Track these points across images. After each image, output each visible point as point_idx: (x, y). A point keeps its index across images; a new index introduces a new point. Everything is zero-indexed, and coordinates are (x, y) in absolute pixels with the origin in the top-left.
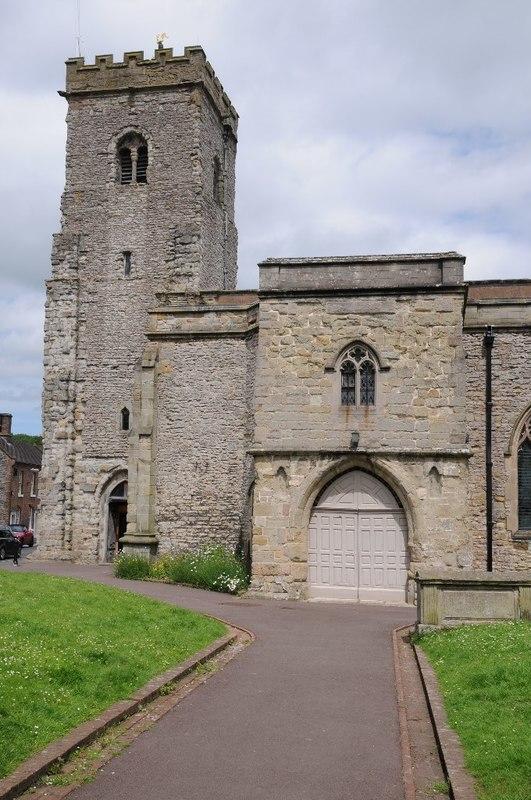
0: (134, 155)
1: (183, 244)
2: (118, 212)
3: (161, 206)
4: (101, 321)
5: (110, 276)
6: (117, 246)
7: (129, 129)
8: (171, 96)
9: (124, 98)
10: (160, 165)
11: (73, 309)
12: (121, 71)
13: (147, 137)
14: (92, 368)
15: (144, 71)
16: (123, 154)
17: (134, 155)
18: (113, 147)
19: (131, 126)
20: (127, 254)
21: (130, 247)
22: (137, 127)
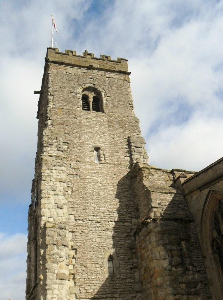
0: (91, 100)
1: (136, 147)
2: (87, 124)
3: (116, 125)
4: (85, 188)
5: (87, 160)
6: (89, 142)
7: (92, 85)
8: (113, 75)
9: (84, 70)
10: (111, 105)
11: (64, 176)
12: (83, 59)
13: (101, 90)
14: (79, 222)
15: (96, 61)
16: (85, 98)
17: (91, 100)
18: (80, 90)
19: (91, 83)
20: (97, 149)
21: (99, 145)
22: (94, 85)
